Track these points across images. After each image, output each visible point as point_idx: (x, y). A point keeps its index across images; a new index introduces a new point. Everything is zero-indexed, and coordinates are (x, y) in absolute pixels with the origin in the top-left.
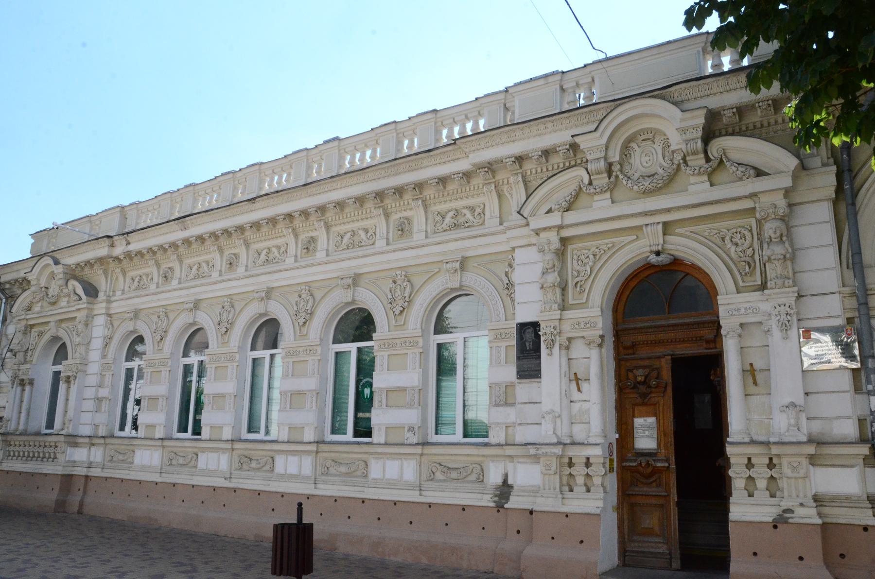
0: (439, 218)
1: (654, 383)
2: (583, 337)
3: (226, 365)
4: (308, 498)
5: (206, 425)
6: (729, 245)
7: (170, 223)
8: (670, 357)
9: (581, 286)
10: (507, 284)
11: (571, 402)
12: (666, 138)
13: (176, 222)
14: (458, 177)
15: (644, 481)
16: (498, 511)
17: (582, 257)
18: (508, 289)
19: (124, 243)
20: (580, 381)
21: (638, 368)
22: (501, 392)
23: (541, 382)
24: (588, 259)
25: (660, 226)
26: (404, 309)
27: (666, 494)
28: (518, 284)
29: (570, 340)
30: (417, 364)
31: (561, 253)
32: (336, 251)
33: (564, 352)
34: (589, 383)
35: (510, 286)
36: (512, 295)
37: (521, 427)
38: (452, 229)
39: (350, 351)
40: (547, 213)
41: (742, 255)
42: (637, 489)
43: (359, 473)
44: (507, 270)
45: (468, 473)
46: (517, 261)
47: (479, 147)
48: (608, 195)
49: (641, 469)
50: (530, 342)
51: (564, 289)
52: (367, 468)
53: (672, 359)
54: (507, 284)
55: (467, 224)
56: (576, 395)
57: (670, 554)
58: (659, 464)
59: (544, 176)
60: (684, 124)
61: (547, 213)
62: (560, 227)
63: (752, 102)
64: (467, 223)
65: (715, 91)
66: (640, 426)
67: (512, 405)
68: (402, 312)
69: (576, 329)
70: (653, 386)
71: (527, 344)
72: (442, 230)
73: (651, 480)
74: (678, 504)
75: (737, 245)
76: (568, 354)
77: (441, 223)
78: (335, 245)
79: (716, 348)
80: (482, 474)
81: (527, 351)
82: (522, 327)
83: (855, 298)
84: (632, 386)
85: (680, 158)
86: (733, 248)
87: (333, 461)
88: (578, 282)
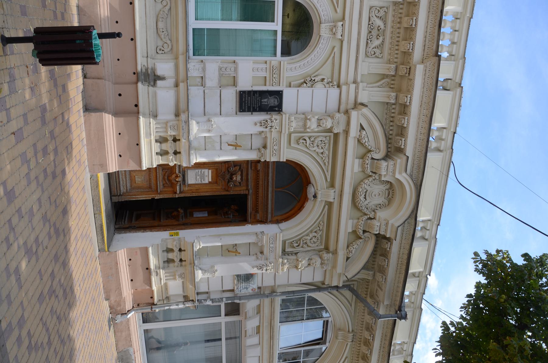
0: (382, 13)
1: (231, 185)
6: (311, 236)
8: (247, 193)
9: (303, 143)
10: (314, 80)
12: (386, 205)
14: (410, 47)
15: (166, 177)
16: (134, 73)
21: (242, 175)
25: (332, 201)
27: (159, 191)
36: (305, 84)
37: (202, 93)
40: (361, 125)
41: (305, 242)
42: (161, 172)
47: (427, 75)
48: (360, 170)
49: (174, 176)
50: (267, 103)
53: (247, 194)
54: (314, 80)
57: (120, 195)
58: (178, 188)
59: (388, 117)
60: (390, 225)
61: (361, 125)
62: (347, 132)
63: (388, 258)
65: (403, 241)
66: (202, 173)
70: (229, 185)
71: (266, 100)
72: (371, 16)
73: (167, 181)
74: (153, 199)
75: (311, 239)
77: (377, 15)
79: (250, 218)
81: (261, 100)
82: (279, 94)
83: (271, 292)
84: (230, 171)
85: (371, 216)
86: (309, 238)
88: (305, 140)
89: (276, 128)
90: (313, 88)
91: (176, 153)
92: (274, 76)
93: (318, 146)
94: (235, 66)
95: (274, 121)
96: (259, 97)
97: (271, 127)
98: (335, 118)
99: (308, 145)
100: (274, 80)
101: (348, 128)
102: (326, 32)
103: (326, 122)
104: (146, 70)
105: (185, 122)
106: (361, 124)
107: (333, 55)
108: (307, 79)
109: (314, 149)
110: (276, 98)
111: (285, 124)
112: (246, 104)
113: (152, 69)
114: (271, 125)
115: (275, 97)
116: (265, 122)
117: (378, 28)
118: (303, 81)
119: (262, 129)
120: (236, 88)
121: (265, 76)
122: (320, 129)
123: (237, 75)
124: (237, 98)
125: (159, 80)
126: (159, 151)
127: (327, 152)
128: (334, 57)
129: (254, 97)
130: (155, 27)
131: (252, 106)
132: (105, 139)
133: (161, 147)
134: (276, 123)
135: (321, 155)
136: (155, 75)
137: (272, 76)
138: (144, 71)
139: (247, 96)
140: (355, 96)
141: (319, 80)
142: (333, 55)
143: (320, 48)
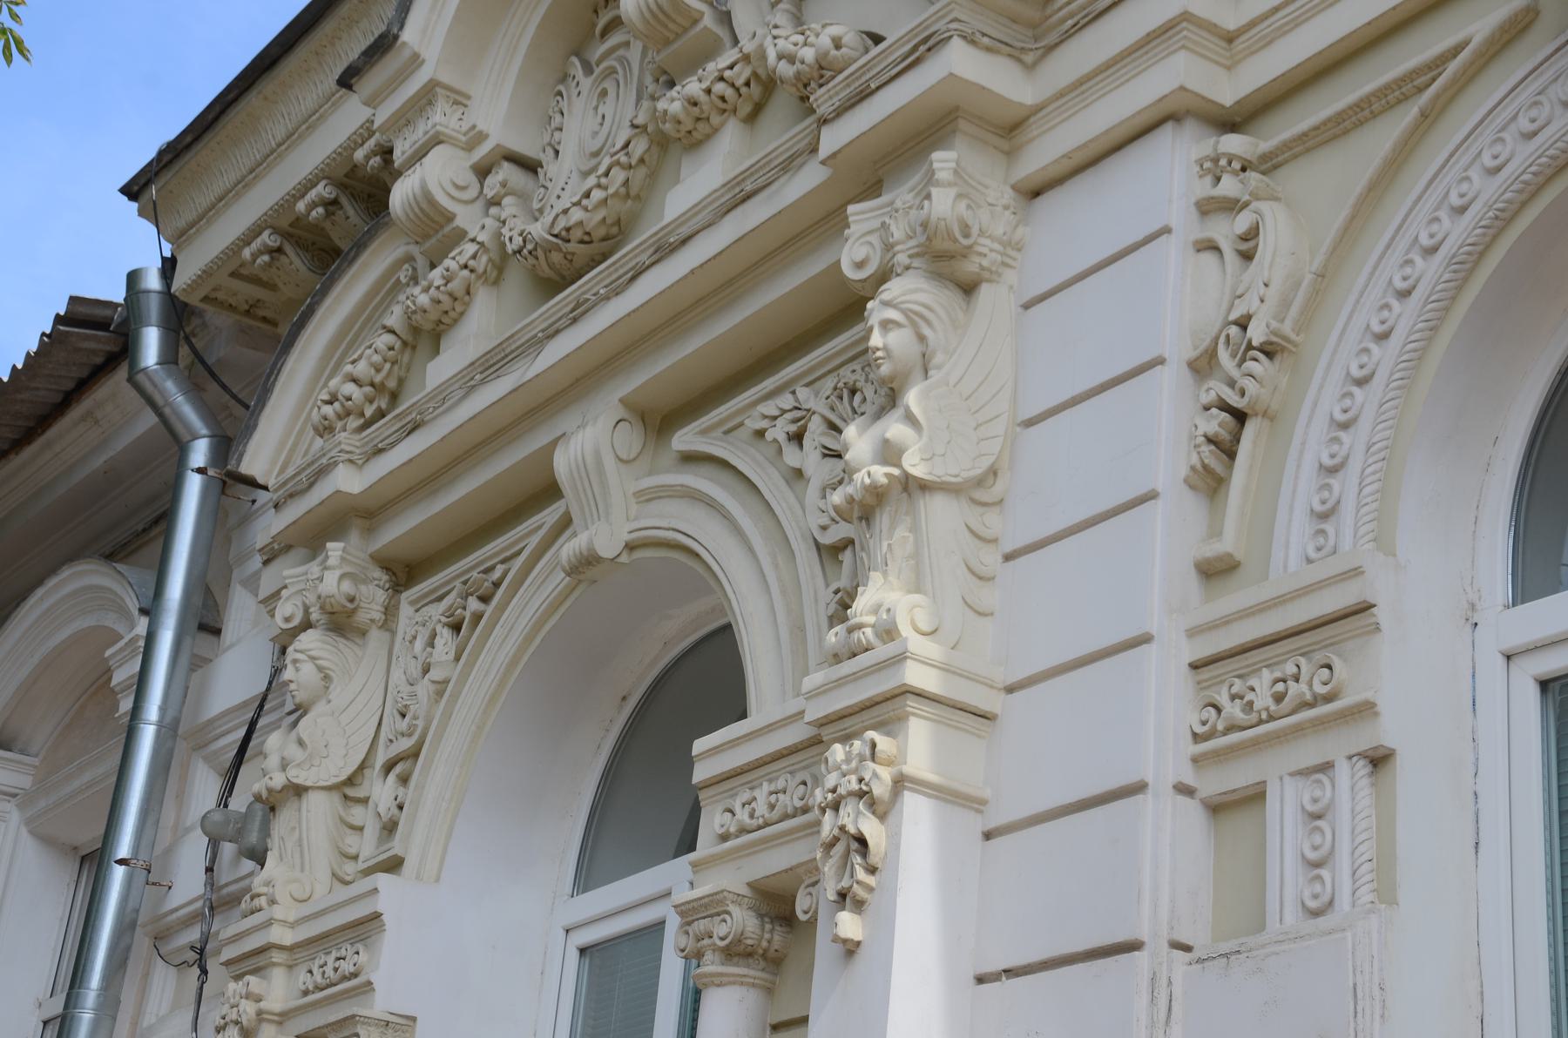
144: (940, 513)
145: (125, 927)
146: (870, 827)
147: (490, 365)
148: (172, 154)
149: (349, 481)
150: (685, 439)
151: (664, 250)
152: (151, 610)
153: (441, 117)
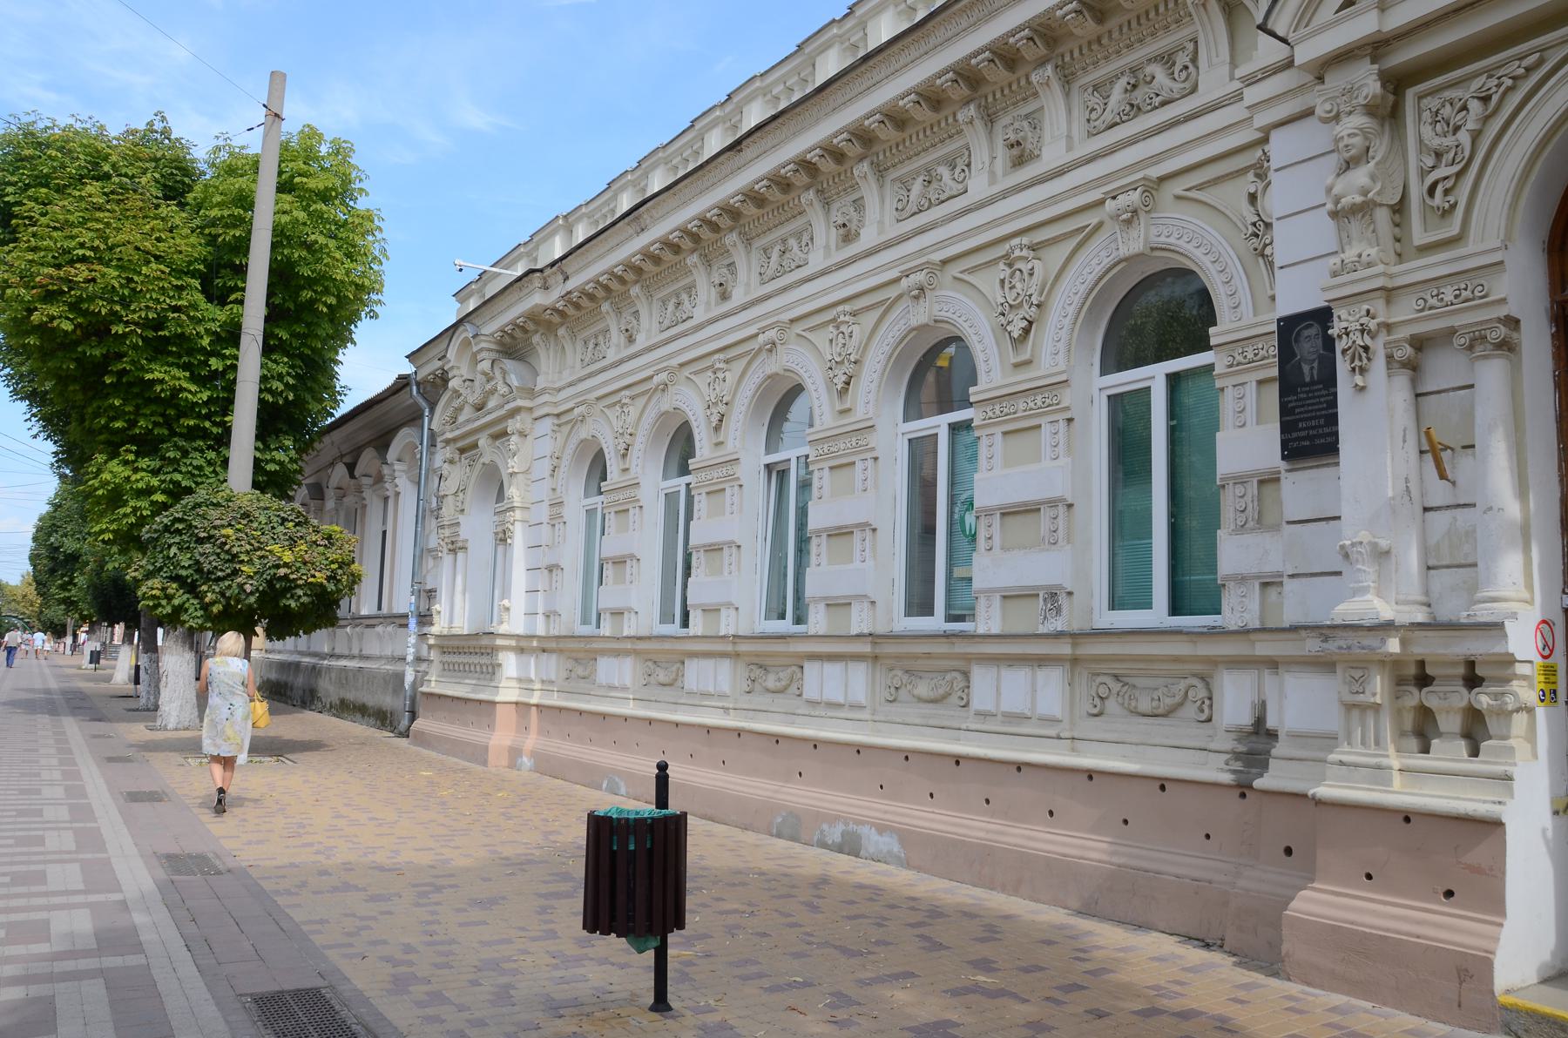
0: (1095, 100)
2: (1452, 332)
3: (721, 486)
4: (815, 746)
5: (696, 607)
7: (618, 225)
9: (1447, 192)
10: (1254, 224)
11: (1426, 509)
13: (626, 220)
17: (1447, 111)
18: (1257, 236)
19: (560, 278)
20: (1446, 455)
22: (1248, 498)
23: (1337, 464)
24: (1465, 112)
26: (1030, 323)
28: (1278, 219)
29: (1420, 344)
30: (1061, 449)
31: (1388, 113)
32: (898, 221)
33: (1402, 380)
34: (1474, 455)
35: (1262, 227)
36: (1268, 251)
37: (1295, 581)
38: (1124, 118)
39: (937, 434)
43: (954, 699)
44: (1252, 191)
45: (1178, 699)
46: (1274, 164)
50: (1314, 360)
51: (1399, 209)
52: (968, 687)
54: (1254, 224)
55: (1157, 101)
56: (1439, 492)
62: (1376, 47)
64: (1158, 95)
67: (1275, 528)
68: (1026, 331)
69: (1430, 308)
71: (1306, 368)
72: (1104, 126)
76: (1414, 382)
78: (897, 209)
80: (1207, 702)
87: (907, 672)
89: (1368, 312)
90: (1274, 221)
91: (1473, 681)
92: (1250, 356)
93: (1457, 129)
94: (1231, 482)
95: (1344, 324)
96: (1296, 394)
97: (1362, 331)
98: (1330, 112)
99: (1456, 168)
100: (1262, 353)
101: (1359, 48)
102: (1136, 236)
103: (1342, 138)
104: (1237, 759)
105: (1326, 640)
106: (1337, 12)
107: (1189, 194)
108: (1251, 248)
109: (1464, 137)
110: (1298, 334)
111: (1352, 282)
112: (1321, 431)
113: (1239, 740)
114: (1358, 334)
115: (1297, 341)
116: (1348, 358)
117: (1132, 91)
118: (1261, 260)
119: (1379, 365)
120: (1283, 472)
121: (1254, 384)
122: (1380, 148)
123: (1252, 476)
124: (1306, 465)
125: (1265, 722)
126: (1462, 746)
127: (1476, 84)
128: (1200, 187)
129: (1297, 410)
130: (1151, 720)
131: (1323, 412)
132: (1368, 930)
133: (1451, 735)
134: (1351, 319)
135: (1495, 98)
136: (1251, 734)
137: (1253, 362)
138: (1239, 763)
139: (1295, 435)
140: (1274, 73)
141: (1252, 209)
142: (1193, 194)
143: (1178, 239)
144: (518, 476)
145: (424, 511)
146: (511, 527)
147: (468, 421)
148: (414, 353)
149: (449, 435)
150: (497, 443)
151: (489, 413)
152: (421, 444)
153: (455, 372)
